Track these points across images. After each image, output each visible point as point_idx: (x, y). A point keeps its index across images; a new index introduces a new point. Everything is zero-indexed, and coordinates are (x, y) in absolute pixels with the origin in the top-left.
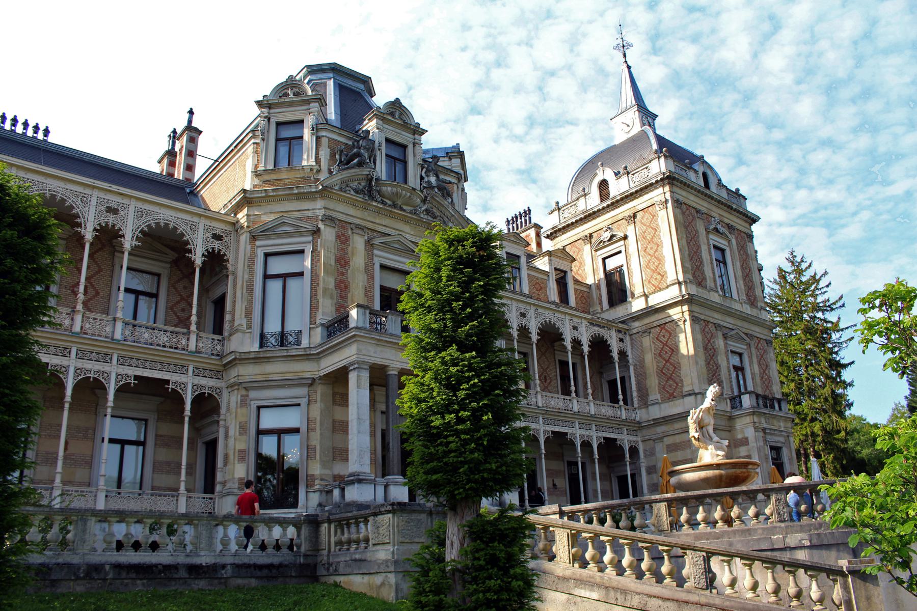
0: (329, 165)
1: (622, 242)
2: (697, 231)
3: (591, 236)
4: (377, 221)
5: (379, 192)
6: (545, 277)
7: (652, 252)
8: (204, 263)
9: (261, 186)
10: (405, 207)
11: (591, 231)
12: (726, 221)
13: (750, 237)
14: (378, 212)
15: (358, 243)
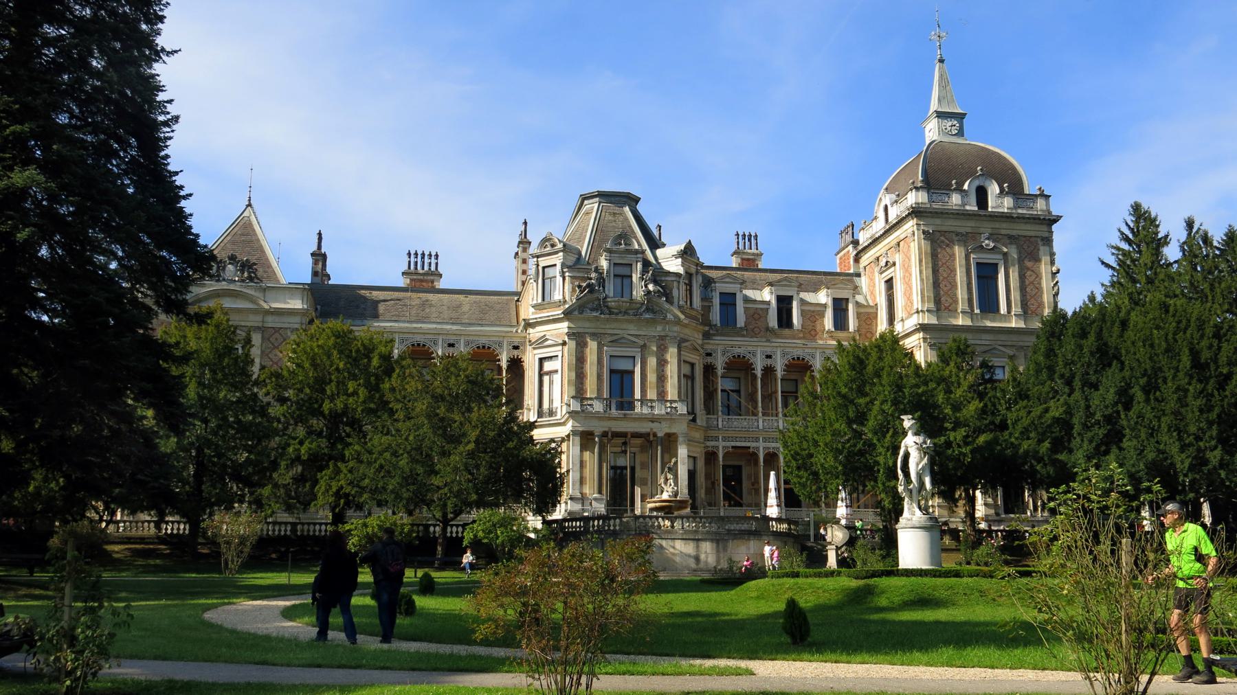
0: (572, 296)
1: (892, 269)
2: (954, 254)
3: (878, 259)
4: (608, 326)
5: (607, 307)
6: (822, 309)
7: (907, 280)
8: (508, 367)
9: (536, 313)
10: (630, 311)
11: (877, 255)
12: (1003, 232)
13: (1048, 241)
14: (607, 320)
15: (592, 346)
